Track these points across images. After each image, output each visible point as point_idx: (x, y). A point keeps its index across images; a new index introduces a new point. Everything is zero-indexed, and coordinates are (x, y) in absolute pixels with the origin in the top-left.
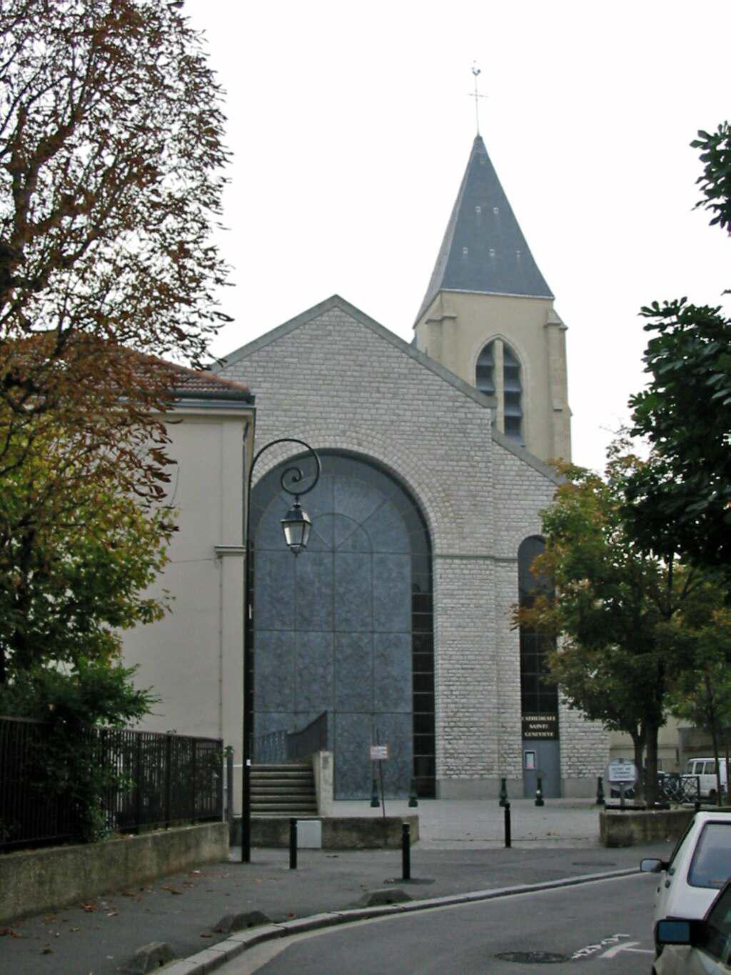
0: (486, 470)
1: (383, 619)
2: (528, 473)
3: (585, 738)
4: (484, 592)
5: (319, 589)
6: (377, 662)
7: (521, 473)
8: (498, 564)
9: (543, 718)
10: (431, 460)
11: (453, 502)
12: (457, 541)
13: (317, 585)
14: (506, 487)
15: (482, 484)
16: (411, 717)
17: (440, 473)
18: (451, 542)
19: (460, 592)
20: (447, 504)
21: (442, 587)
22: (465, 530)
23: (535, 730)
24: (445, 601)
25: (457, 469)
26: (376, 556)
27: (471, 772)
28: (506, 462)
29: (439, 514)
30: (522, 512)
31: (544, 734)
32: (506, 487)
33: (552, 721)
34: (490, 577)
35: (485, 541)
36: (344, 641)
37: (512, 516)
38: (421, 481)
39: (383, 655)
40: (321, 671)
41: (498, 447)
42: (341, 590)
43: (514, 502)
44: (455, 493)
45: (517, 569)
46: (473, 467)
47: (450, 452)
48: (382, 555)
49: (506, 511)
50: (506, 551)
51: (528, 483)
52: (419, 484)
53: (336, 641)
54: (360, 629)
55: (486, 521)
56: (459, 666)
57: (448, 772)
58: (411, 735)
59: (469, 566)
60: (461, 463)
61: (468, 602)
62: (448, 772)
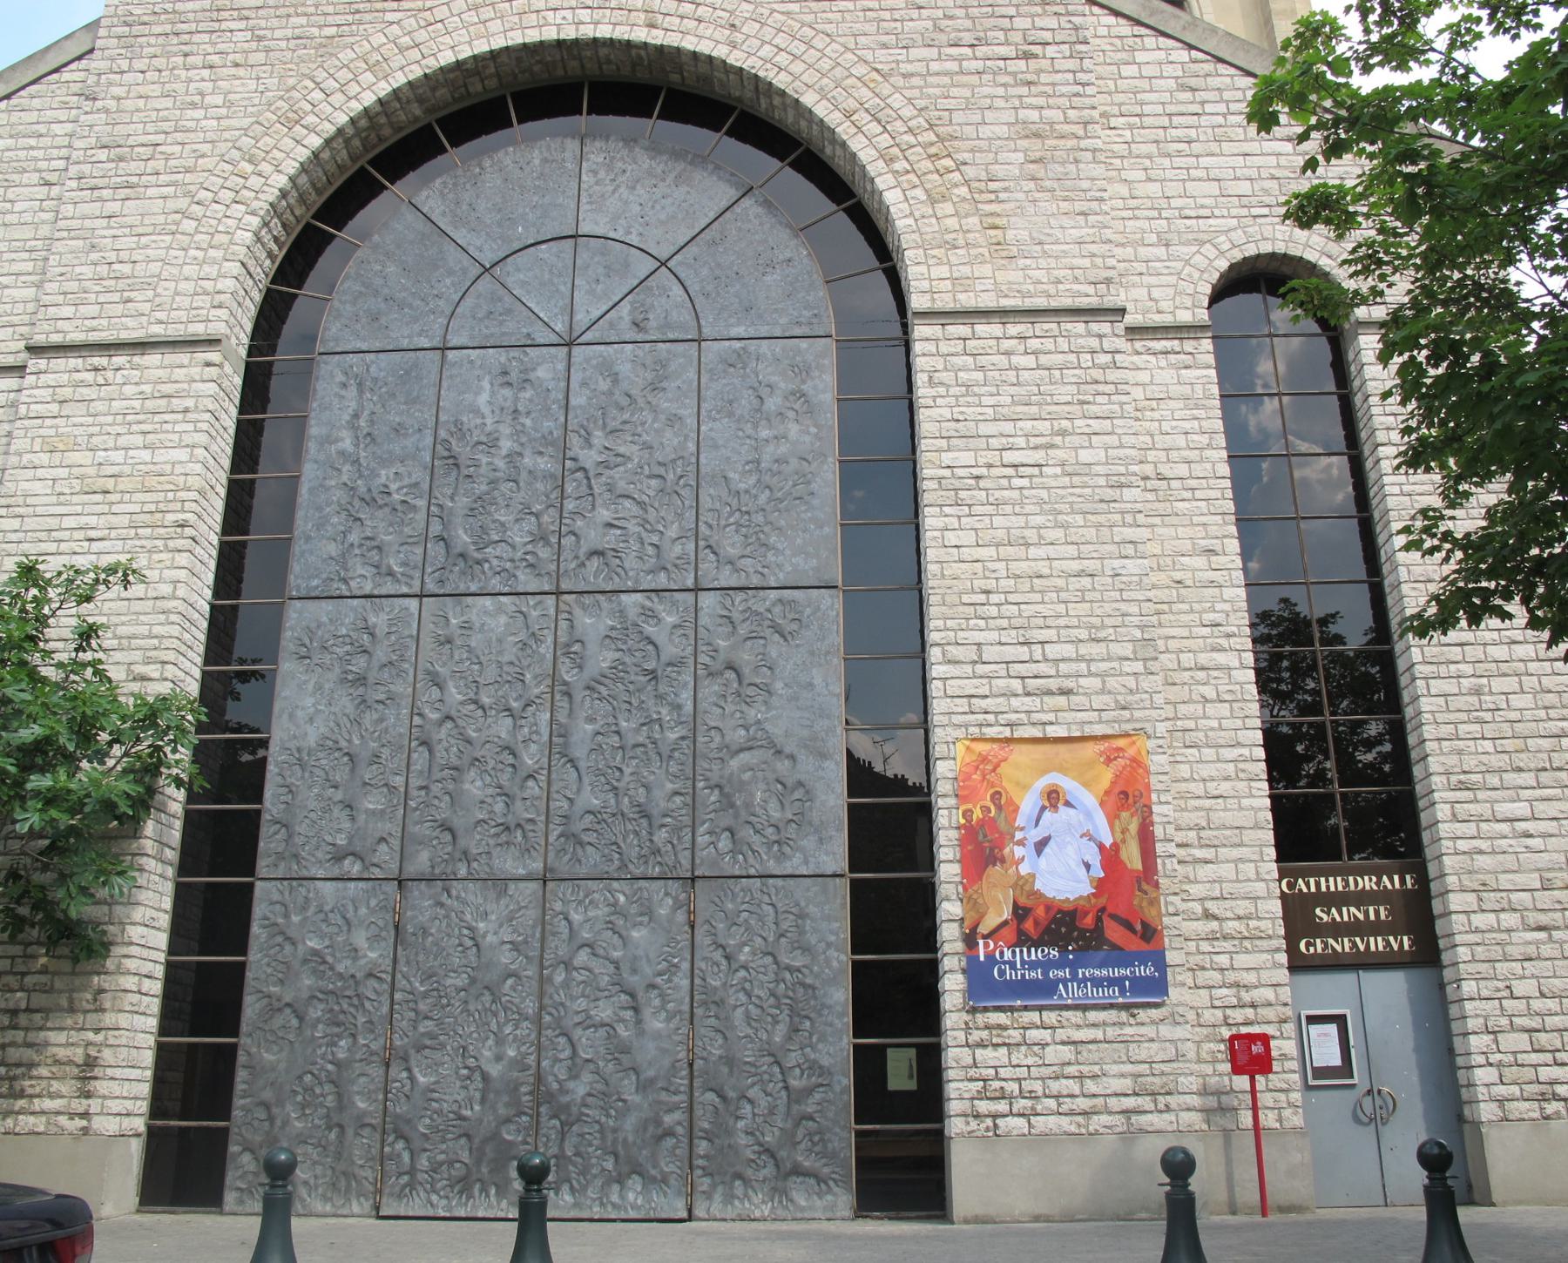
0: (1071, 64)
1: (731, 545)
2: (1214, 82)
3: (1546, 951)
4: (1096, 425)
5: (512, 457)
6: (710, 689)
7: (1193, 82)
8: (1138, 345)
9: (1367, 883)
10: (885, 46)
11: (967, 156)
12: (986, 270)
13: (506, 445)
14: (1147, 121)
15: (1064, 102)
16: (843, 889)
17: (916, 81)
18: (966, 270)
19: (1008, 427)
20: (948, 162)
21: (934, 413)
22: (1010, 234)
23: (1337, 930)
24: (947, 458)
25: (979, 65)
26: (712, 349)
27: (1083, 1103)
28: (1141, 57)
29: (920, 193)
30: (1213, 188)
31: (1377, 944)
32: (1147, 121)
33: (1404, 892)
34: (1112, 375)
35: (1086, 262)
36: (592, 623)
37: (1175, 203)
38: (852, 104)
39: (731, 667)
40: (502, 728)
41: (1112, 20)
42: (589, 458)
43: (1178, 162)
44: (969, 131)
45: (1211, 359)
46: (1027, 56)
47: (944, 23)
48: (737, 345)
49: (1154, 189)
50: (1164, 305)
51: (1222, 108)
52: (848, 115)
53: (563, 625)
54: (648, 582)
55: (1078, 206)
56: (1016, 685)
57: (983, 1106)
58: (840, 959)
59: (1034, 344)
60: (981, 51)
61: (1038, 456)
62: (983, 1106)
